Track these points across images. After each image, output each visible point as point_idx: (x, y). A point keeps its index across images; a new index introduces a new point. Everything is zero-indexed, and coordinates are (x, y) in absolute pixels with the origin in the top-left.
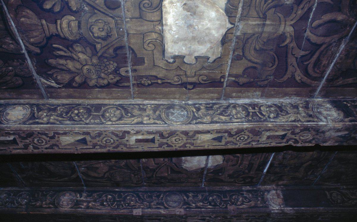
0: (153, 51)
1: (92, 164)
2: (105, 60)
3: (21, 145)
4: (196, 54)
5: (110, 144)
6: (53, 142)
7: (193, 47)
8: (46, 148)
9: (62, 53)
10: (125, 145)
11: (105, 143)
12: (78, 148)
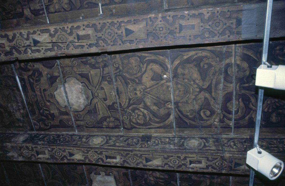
0: (120, 179)
1: (156, 84)
2: (141, 175)
3: (188, 160)
4: (100, 176)
5: (131, 157)
6: (166, 161)
7: (103, 179)
8: (172, 156)
9: (161, 181)
10: (122, 155)
11: (135, 158)
12: (151, 155)
